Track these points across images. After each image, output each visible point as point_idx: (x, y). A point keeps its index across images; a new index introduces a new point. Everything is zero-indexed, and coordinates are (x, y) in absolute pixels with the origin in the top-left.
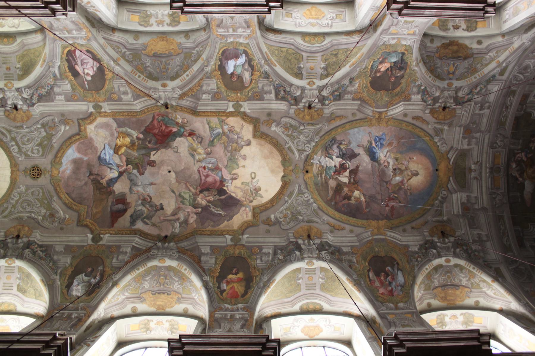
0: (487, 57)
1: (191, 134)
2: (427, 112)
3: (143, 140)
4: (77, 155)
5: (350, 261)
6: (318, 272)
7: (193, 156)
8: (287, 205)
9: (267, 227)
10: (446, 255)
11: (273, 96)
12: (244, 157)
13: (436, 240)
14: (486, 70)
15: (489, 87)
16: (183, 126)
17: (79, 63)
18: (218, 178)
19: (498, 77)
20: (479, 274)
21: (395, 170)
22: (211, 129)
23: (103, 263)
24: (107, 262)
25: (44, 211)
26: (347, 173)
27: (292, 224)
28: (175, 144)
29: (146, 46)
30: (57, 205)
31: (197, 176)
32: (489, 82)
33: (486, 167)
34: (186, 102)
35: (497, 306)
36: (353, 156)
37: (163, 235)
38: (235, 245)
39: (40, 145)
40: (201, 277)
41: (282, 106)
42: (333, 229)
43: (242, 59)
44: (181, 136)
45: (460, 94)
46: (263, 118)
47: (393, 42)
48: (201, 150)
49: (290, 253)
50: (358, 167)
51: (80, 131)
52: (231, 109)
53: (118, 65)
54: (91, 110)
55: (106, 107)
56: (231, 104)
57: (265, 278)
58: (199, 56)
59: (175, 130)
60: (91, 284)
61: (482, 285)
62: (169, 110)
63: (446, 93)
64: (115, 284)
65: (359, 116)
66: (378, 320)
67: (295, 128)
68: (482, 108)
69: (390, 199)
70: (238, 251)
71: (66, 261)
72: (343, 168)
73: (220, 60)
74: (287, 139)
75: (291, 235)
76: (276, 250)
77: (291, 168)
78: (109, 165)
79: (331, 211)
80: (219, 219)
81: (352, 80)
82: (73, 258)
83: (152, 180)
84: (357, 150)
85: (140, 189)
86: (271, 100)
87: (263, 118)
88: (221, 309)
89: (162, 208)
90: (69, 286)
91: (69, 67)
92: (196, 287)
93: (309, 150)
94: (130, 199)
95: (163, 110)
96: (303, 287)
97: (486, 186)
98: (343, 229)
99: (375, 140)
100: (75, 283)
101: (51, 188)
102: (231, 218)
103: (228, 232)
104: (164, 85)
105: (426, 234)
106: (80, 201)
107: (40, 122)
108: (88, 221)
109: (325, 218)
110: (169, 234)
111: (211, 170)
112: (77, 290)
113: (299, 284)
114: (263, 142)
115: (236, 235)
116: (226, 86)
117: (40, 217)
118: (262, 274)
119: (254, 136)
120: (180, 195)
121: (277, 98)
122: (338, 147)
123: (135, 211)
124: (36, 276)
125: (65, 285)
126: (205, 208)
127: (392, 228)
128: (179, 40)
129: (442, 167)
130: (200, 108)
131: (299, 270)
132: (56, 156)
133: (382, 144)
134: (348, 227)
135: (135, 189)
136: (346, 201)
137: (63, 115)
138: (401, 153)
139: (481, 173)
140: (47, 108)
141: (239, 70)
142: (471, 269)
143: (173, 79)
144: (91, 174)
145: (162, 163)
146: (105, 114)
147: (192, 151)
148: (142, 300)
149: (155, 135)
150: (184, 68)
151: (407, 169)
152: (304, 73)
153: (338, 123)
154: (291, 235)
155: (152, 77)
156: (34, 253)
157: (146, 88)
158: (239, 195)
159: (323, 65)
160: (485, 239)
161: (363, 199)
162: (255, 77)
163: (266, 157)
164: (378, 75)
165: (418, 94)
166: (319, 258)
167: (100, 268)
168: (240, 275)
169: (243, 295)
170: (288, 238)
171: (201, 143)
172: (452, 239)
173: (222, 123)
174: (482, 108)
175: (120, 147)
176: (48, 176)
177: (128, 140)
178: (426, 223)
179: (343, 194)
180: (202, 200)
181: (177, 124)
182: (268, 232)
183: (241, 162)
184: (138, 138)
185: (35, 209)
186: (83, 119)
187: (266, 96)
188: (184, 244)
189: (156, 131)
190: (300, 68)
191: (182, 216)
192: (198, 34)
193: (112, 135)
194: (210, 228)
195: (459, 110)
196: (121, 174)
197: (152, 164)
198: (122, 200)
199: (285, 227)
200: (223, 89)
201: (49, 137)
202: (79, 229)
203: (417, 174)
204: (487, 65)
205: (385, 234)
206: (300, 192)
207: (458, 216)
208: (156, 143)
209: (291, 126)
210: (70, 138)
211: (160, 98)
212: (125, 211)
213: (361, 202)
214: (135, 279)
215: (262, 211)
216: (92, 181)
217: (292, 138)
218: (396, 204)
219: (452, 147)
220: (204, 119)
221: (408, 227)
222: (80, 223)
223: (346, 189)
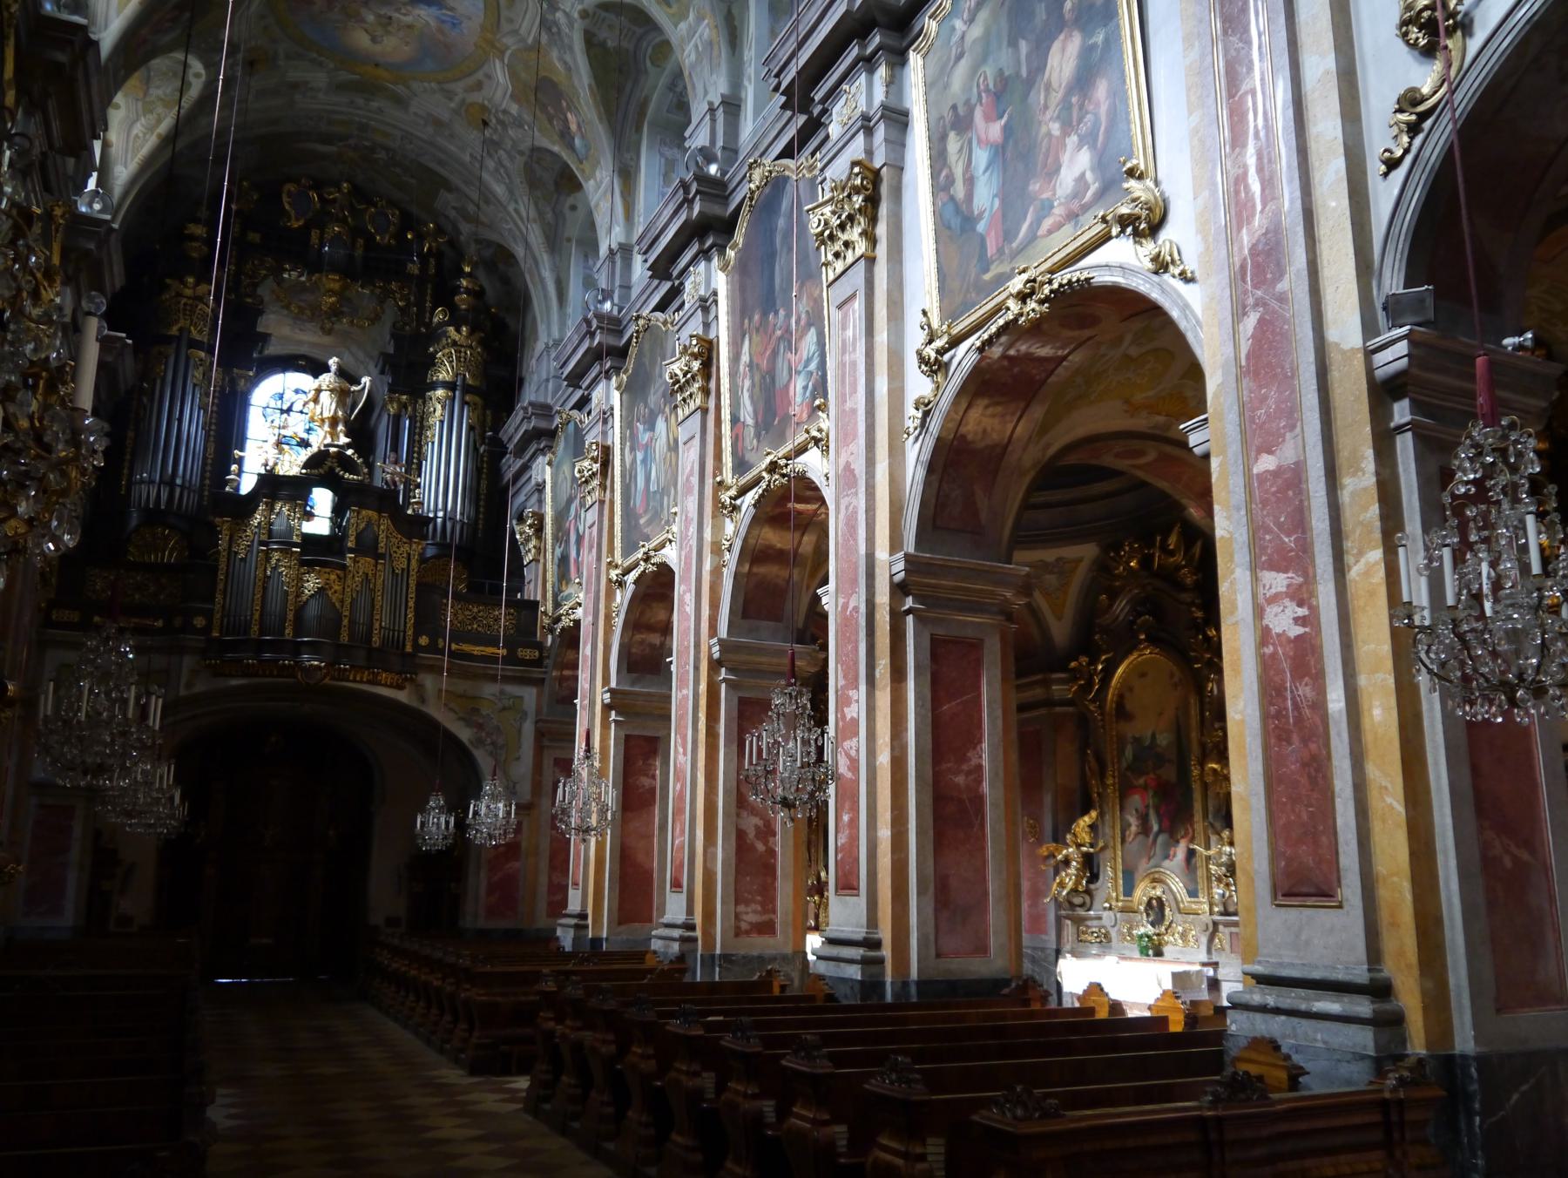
0: (548, 209)
2: (486, 102)
15: (503, 186)
20: (172, 115)
45: (501, 152)
61: (152, 118)
164: (564, 104)
204: (536, 205)
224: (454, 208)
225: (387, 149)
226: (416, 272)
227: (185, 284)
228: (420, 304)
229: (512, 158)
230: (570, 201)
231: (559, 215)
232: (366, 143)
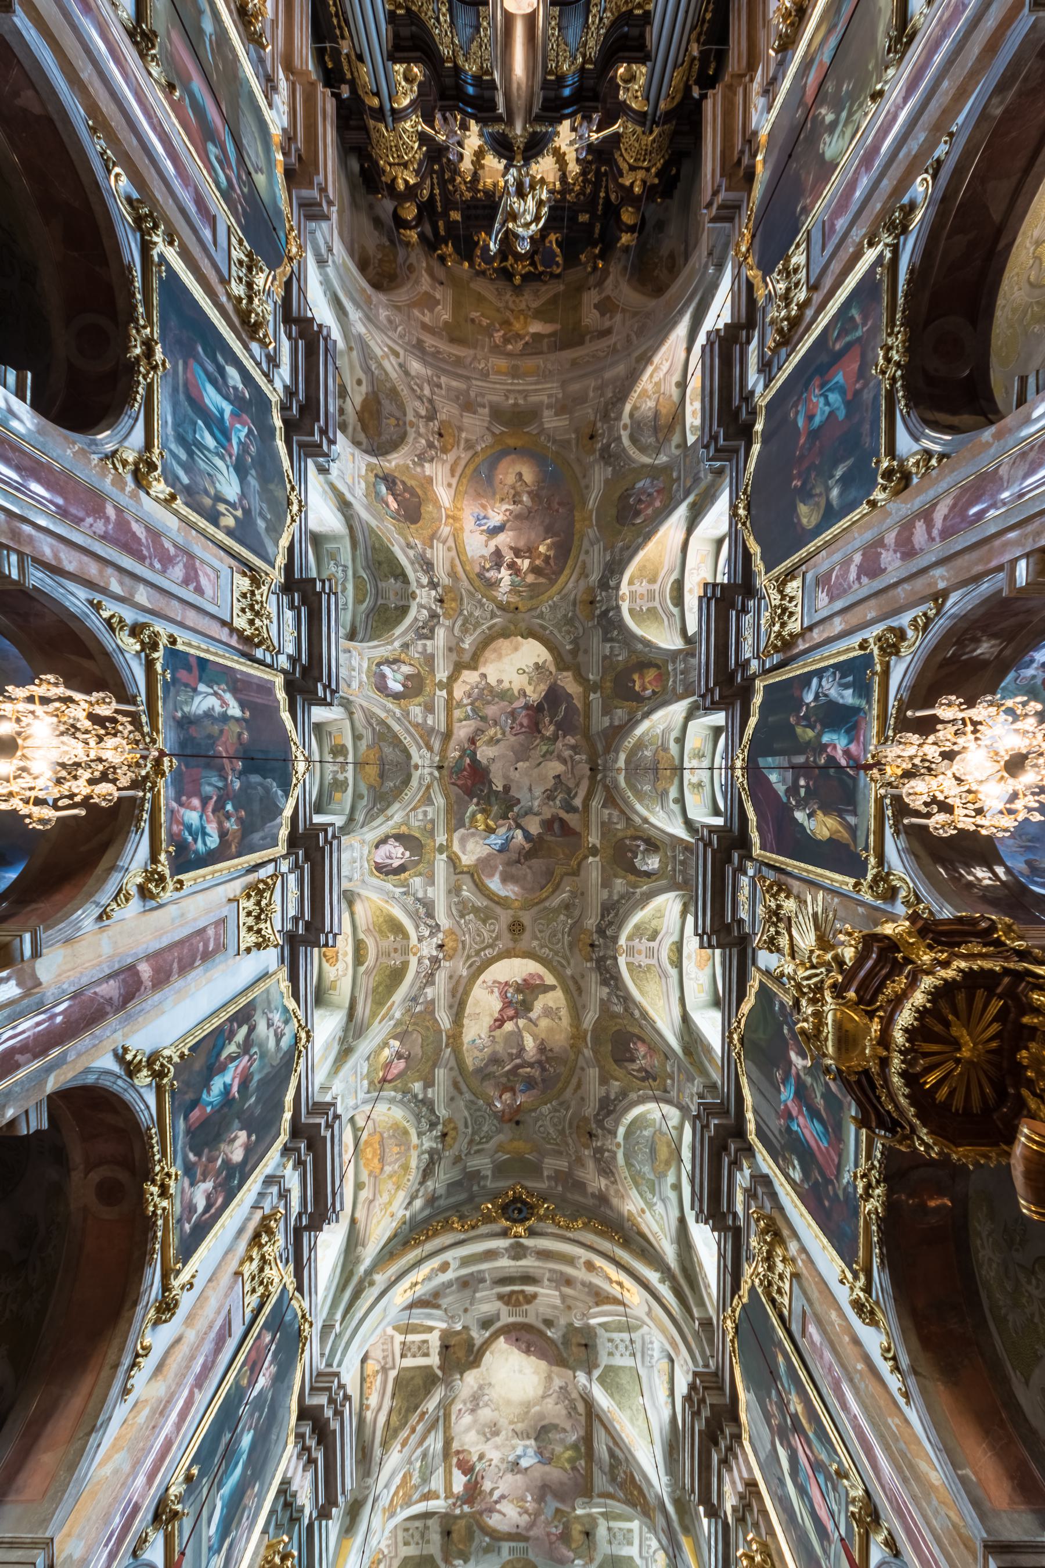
0: (376, 372)
1: (472, 741)
3: (479, 800)
4: (497, 878)
5: (622, 550)
6: (633, 588)
7: (498, 741)
8: (556, 632)
9: (580, 653)
10: (618, 430)
11: (429, 643)
12: (500, 682)
13: (599, 445)
14: (393, 375)
15: (413, 373)
16: (463, 751)
17: (389, 861)
18: (524, 712)
19: (401, 360)
21: (514, 503)
22: (467, 718)
23: (623, 839)
24: (620, 835)
25: (562, 917)
26: (519, 561)
27: (577, 624)
28: (484, 761)
29: (371, 787)
30: (556, 902)
31: (522, 737)
32: (407, 373)
33: (512, 384)
34: (437, 746)
35: (683, 355)
36: (498, 553)
37: (588, 773)
38: (601, 688)
39: (484, 922)
40: (638, 722)
41: (441, 633)
42: (584, 574)
43: (386, 669)
44: (474, 753)
45: (423, 413)
46: (454, 657)
47: (363, 485)
48: (492, 732)
49: (610, 622)
50: (511, 548)
51: (468, 873)
52: (444, 693)
53: (392, 816)
54: (444, 856)
55: (441, 839)
56: (438, 693)
57: (640, 646)
58: (382, 723)
59: (468, 761)
60: (646, 850)
62: (446, 765)
63: (422, 430)
64: (646, 821)
65: (451, 542)
66: (691, 499)
67: (466, 621)
68: (439, 386)
69: (549, 507)
70: (608, 684)
71: (619, 884)
72: (512, 566)
73: (388, 696)
74: (479, 631)
75: (590, 624)
76: (606, 639)
77: (512, 627)
78: (508, 840)
79: (562, 579)
80: (571, 709)
81: (409, 546)
82: (616, 876)
83: (526, 790)
84: (492, 548)
85: (536, 803)
86: (433, 645)
87: (454, 657)
88: (674, 689)
89: (559, 776)
90: (648, 874)
92: (650, 728)
93: (492, 606)
94: (547, 814)
95: (445, 772)
96: (651, 605)
97: (536, 384)
98: (584, 563)
99: (480, 525)
100: (645, 868)
101: (536, 909)
102: (570, 695)
103: (586, 697)
104: (416, 767)
105: (592, 459)
106: (549, 874)
108: (574, 863)
109: (570, 585)
110: (588, 767)
111: (514, 720)
112: (653, 863)
113: (648, 610)
114: (482, 659)
115: (589, 687)
116: (417, 696)
118: (635, 652)
119: (475, 669)
120: (544, 756)
121: (432, 638)
122: (488, 570)
123: (562, 808)
124: (637, 918)
125: (646, 879)
126: (559, 726)
127: (584, 502)
128: (364, 747)
129: (511, 442)
130: (443, 728)
131: (631, 611)
132: (498, 903)
133: (485, 518)
134: (582, 557)
135: (536, 809)
136: (552, 562)
137: (449, 892)
138: (494, 494)
139: (519, 391)
141: (400, 677)
142: (636, 395)
143: (409, 757)
144: (518, 862)
145: (506, 777)
146: (450, 840)
147: (493, 741)
148: (664, 793)
149: (473, 785)
150: (396, 742)
151: (513, 487)
152: (402, 603)
153: (459, 569)
154: (590, 624)
155: (407, 781)
156: (611, 923)
157: (419, 789)
158: (543, 688)
159: (392, 580)
160: (600, 381)
161: (549, 541)
162: (407, 660)
163: (500, 657)
165: (423, 466)
166: (618, 587)
167: (628, 842)
168: (636, 677)
169: (658, 667)
170: (594, 627)
171: (483, 732)
172: (599, 424)
173: (460, 705)
174: (439, 386)
175: (487, 826)
176: (521, 913)
177: (479, 816)
178: (578, 460)
179: (543, 565)
180: (549, 731)
181: (461, 757)
182: (586, 652)
183: (506, 685)
184: (477, 804)
185: (560, 927)
186: (455, 868)
187: (429, 650)
188: (600, 747)
189: (469, 782)
190: (396, 608)
191: (567, 753)
192: (357, 724)
193: (473, 835)
194: (581, 719)
195: (442, 416)
196: (519, 826)
197: (507, 788)
198: (548, 825)
199: (581, 631)
200: (420, 699)
201: (476, 910)
202: (582, 873)
203: (520, 475)
204: (387, 374)
205: (591, 511)
206: (541, 616)
207: (571, 420)
208: (483, 784)
209: (463, 625)
210: (476, 885)
211: (431, 774)
212: (561, 820)
213: (553, 544)
214: (640, 801)
215: (562, 660)
216: (526, 859)
217: (477, 625)
218: (557, 500)
219: (488, 429)
220: (456, 725)
221: (583, 483)
222: (576, 873)
223: (537, 562)
224: (438, 303)
225: (496, 349)
226: (452, 213)
227: (644, 182)
228: (443, 183)
229: (418, 415)
230: (364, 389)
231: (367, 370)
232: (510, 347)
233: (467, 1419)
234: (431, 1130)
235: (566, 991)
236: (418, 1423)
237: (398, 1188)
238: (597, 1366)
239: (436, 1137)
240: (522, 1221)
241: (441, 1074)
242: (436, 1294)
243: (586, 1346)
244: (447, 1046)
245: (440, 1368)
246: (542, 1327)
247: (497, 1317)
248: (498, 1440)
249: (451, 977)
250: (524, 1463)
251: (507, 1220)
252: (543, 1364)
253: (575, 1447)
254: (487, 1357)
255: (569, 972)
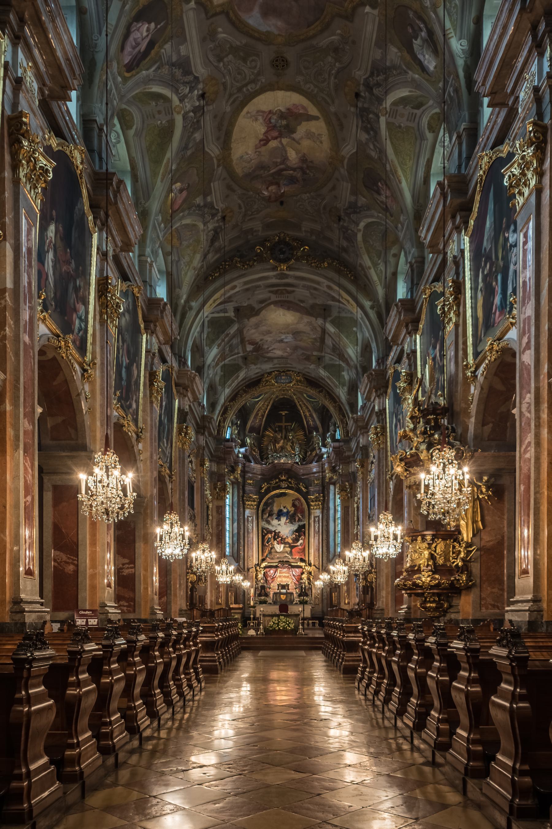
25: (330, 59)
91: (144, 59)
107: (216, 64)
117: (337, 64)
140: (198, 61)
233: (253, 331)
234: (213, 218)
235: (329, 123)
236: (225, 338)
237: (195, 253)
238: (330, 316)
239: (218, 221)
240: (285, 261)
241: (216, 186)
242: (230, 297)
243: (325, 310)
244: (218, 166)
245: (235, 317)
246: (298, 302)
247: (270, 298)
248: (271, 335)
249: (215, 117)
250: (285, 340)
251: (274, 259)
252: (298, 314)
253: (315, 339)
254: (263, 312)
255: (332, 109)
